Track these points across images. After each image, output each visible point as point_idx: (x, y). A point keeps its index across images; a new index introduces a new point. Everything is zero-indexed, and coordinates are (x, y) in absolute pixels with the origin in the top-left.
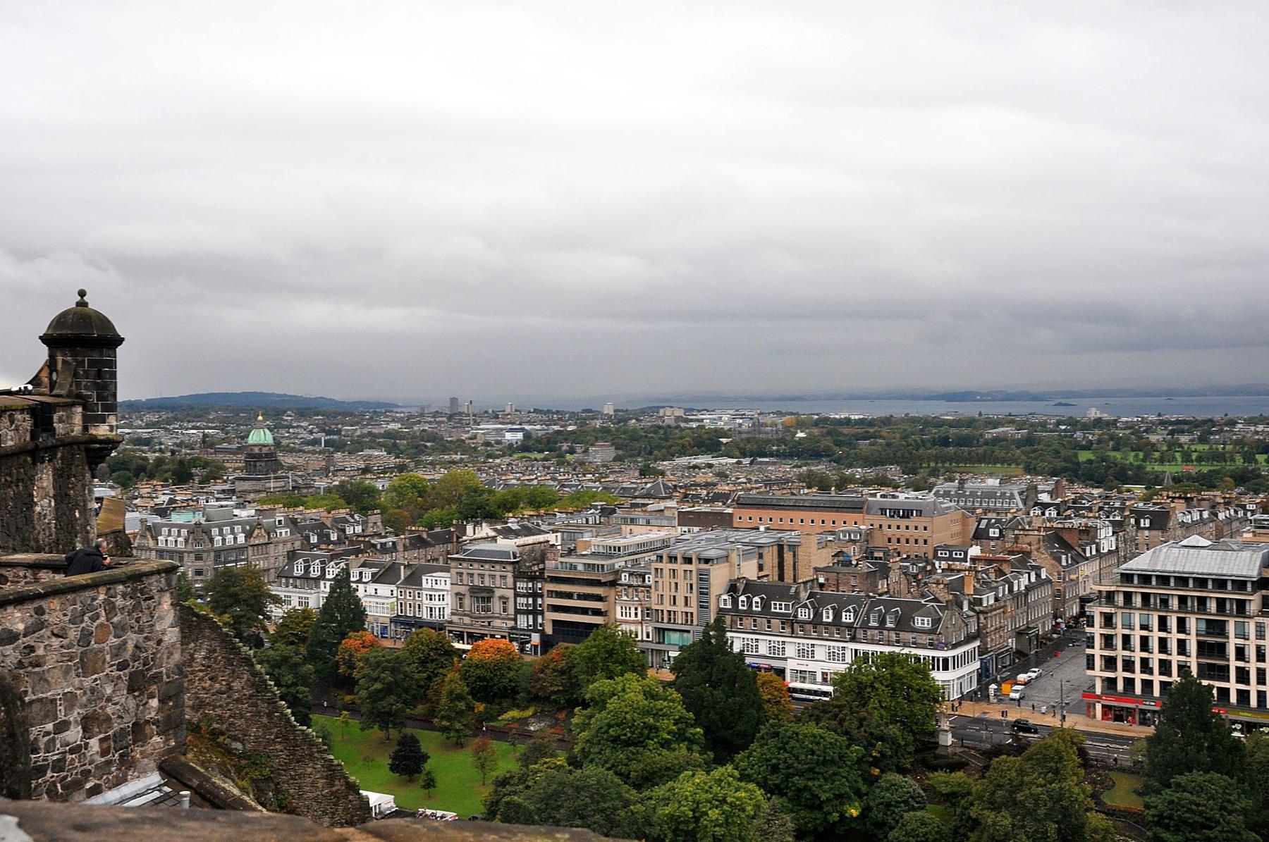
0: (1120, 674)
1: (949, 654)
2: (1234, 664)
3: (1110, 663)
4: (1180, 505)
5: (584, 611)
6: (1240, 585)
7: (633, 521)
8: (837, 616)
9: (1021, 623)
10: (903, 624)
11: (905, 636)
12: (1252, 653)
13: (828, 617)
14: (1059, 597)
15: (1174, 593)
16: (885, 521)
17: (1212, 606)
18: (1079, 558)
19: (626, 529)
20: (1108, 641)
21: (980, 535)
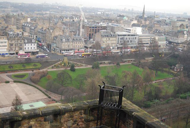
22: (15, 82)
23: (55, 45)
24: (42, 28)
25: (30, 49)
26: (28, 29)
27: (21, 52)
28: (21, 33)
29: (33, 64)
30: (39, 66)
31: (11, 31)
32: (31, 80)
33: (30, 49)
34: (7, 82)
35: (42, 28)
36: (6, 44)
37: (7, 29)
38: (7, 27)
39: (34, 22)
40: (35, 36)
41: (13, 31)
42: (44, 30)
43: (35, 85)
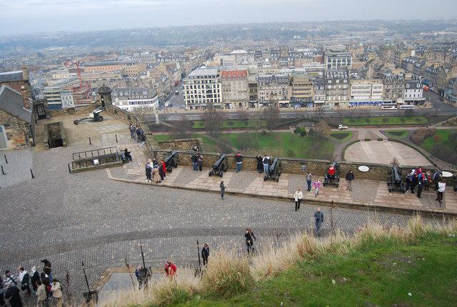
0: (191, 99)
1: (152, 100)
2: (213, 94)
3: (189, 97)
4: (191, 55)
5: (55, 101)
6: (214, 77)
7: (55, 73)
8: (124, 94)
9: (164, 90)
10: (140, 93)
11: (142, 97)
12: (217, 91)
13: (121, 94)
14: (171, 82)
15: (200, 80)
16: (125, 66)
17: (208, 82)
18: (173, 72)
19: (54, 76)
20: (188, 92)
21: (148, 68)
22: (389, 140)
23: (450, 92)
24: (433, 66)
25: (412, 96)
26: (410, 67)
27: (400, 101)
28: (402, 75)
29: (415, 118)
30: (424, 121)
31: (388, 72)
32: (411, 139)
33: (412, 96)
34: (380, 140)
35: (433, 66)
36: (381, 90)
37: (382, 69)
38: (383, 65)
39: (420, 56)
40: (420, 77)
41: (390, 71)
42: (435, 68)
43: (419, 148)
